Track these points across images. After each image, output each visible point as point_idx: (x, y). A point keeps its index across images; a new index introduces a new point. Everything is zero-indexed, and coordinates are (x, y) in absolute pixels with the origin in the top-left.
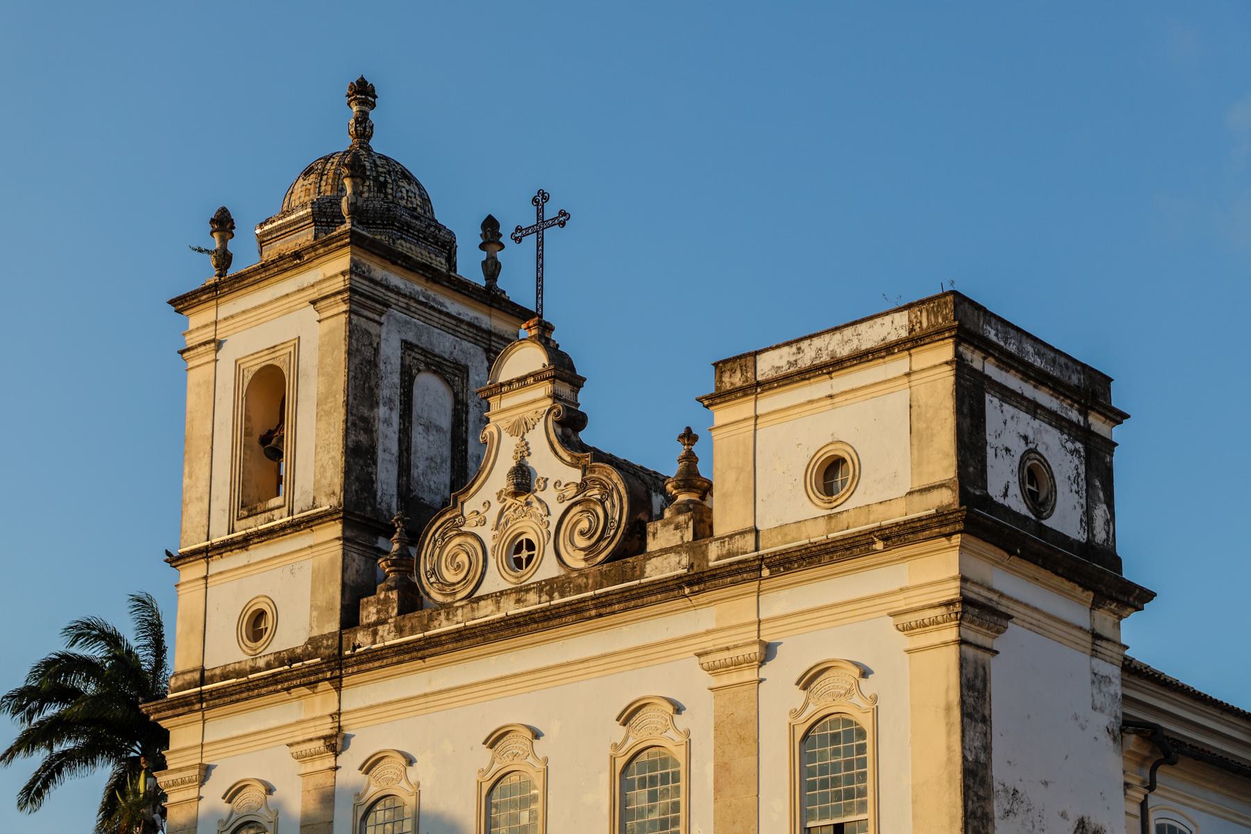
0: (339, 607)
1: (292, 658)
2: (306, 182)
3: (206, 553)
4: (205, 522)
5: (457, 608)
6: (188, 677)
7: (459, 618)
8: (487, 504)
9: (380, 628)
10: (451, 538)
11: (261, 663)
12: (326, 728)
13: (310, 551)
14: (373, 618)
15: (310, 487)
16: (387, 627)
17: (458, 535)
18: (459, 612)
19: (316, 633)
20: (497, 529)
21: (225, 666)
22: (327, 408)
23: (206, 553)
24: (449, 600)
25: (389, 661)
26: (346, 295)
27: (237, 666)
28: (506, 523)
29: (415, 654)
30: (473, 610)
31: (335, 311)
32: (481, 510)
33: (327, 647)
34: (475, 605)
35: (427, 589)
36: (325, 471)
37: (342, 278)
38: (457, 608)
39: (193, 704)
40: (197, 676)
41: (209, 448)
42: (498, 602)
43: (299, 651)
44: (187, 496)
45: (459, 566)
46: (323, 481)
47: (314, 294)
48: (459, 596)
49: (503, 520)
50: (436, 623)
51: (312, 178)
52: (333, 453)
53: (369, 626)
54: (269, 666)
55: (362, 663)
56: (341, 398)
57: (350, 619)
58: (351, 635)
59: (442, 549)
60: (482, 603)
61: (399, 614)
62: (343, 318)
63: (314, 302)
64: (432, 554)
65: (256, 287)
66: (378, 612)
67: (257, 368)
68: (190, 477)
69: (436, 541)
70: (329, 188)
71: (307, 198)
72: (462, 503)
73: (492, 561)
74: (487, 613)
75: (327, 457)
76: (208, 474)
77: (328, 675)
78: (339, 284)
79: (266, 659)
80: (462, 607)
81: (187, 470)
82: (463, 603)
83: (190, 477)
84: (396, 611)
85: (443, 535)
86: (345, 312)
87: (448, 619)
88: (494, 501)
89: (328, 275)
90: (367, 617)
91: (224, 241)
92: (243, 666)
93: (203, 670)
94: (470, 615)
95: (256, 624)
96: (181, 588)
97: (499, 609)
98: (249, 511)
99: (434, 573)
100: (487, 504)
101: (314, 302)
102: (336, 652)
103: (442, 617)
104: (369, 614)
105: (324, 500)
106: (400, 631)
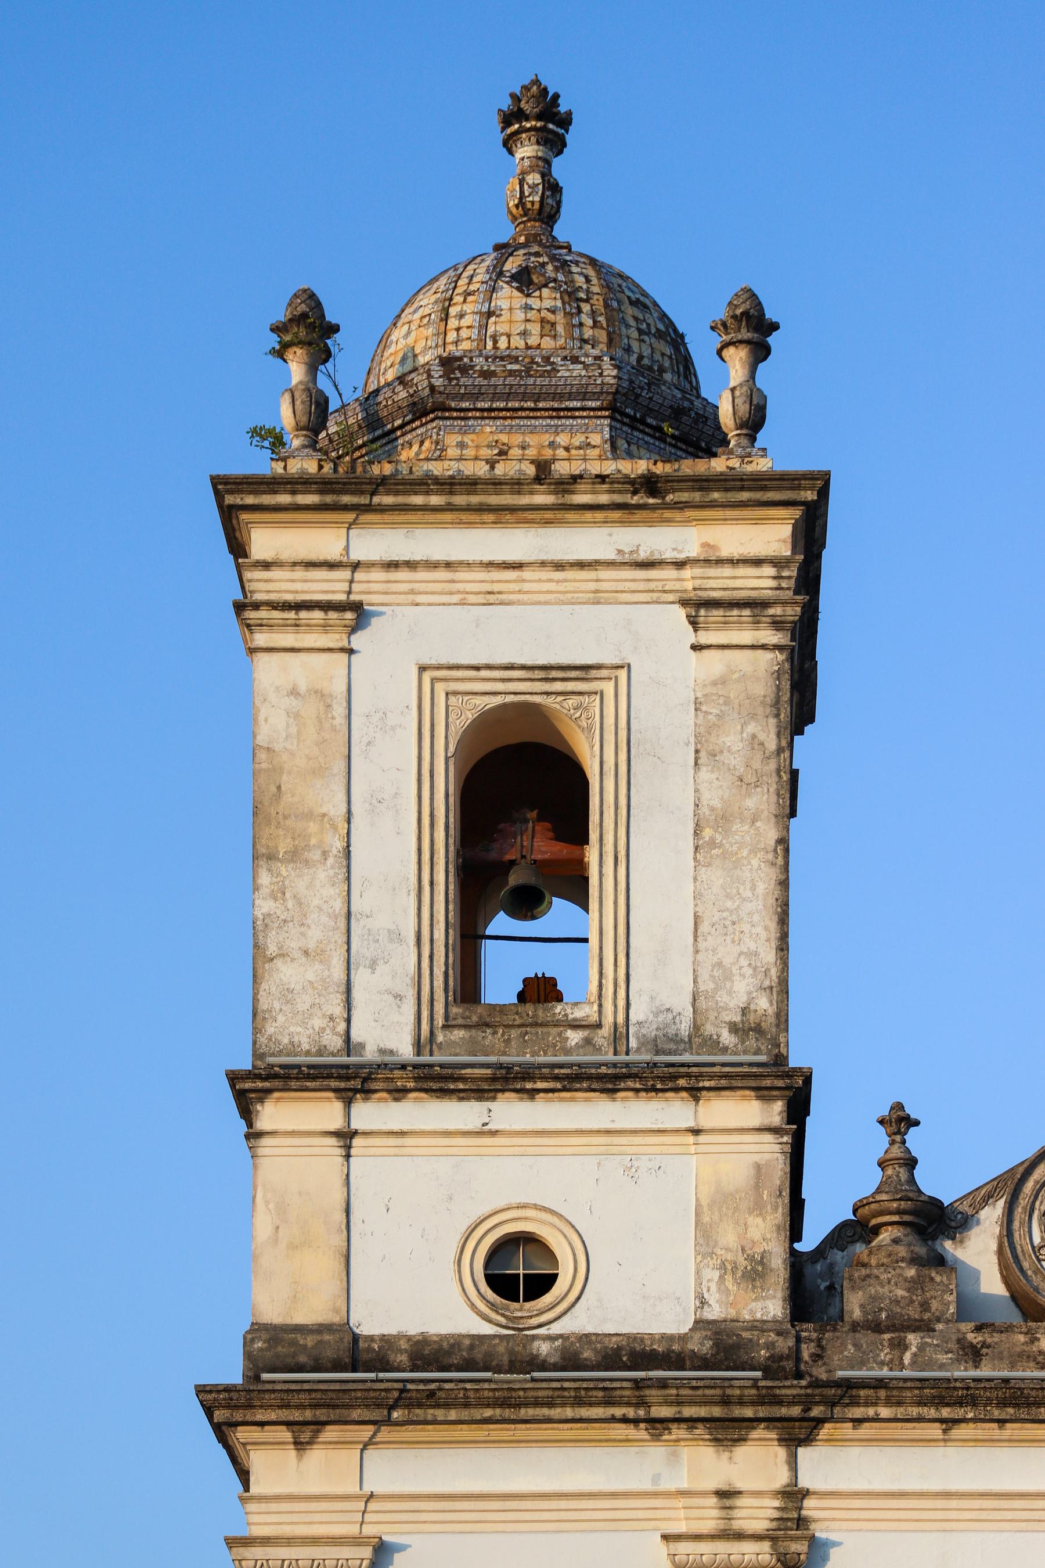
2: (534, 303)
3: (351, 1078)
4: (339, 1011)
15: (682, 1004)
23: (351, 1078)
31: (746, 637)
36: (728, 977)
46: (723, 998)
51: (548, 299)
70: (602, 335)
71: (548, 343)
75: (736, 950)
78: (760, 582)
91: (313, 369)
95: (517, 1269)
96: (265, 1141)
105: (727, 1038)
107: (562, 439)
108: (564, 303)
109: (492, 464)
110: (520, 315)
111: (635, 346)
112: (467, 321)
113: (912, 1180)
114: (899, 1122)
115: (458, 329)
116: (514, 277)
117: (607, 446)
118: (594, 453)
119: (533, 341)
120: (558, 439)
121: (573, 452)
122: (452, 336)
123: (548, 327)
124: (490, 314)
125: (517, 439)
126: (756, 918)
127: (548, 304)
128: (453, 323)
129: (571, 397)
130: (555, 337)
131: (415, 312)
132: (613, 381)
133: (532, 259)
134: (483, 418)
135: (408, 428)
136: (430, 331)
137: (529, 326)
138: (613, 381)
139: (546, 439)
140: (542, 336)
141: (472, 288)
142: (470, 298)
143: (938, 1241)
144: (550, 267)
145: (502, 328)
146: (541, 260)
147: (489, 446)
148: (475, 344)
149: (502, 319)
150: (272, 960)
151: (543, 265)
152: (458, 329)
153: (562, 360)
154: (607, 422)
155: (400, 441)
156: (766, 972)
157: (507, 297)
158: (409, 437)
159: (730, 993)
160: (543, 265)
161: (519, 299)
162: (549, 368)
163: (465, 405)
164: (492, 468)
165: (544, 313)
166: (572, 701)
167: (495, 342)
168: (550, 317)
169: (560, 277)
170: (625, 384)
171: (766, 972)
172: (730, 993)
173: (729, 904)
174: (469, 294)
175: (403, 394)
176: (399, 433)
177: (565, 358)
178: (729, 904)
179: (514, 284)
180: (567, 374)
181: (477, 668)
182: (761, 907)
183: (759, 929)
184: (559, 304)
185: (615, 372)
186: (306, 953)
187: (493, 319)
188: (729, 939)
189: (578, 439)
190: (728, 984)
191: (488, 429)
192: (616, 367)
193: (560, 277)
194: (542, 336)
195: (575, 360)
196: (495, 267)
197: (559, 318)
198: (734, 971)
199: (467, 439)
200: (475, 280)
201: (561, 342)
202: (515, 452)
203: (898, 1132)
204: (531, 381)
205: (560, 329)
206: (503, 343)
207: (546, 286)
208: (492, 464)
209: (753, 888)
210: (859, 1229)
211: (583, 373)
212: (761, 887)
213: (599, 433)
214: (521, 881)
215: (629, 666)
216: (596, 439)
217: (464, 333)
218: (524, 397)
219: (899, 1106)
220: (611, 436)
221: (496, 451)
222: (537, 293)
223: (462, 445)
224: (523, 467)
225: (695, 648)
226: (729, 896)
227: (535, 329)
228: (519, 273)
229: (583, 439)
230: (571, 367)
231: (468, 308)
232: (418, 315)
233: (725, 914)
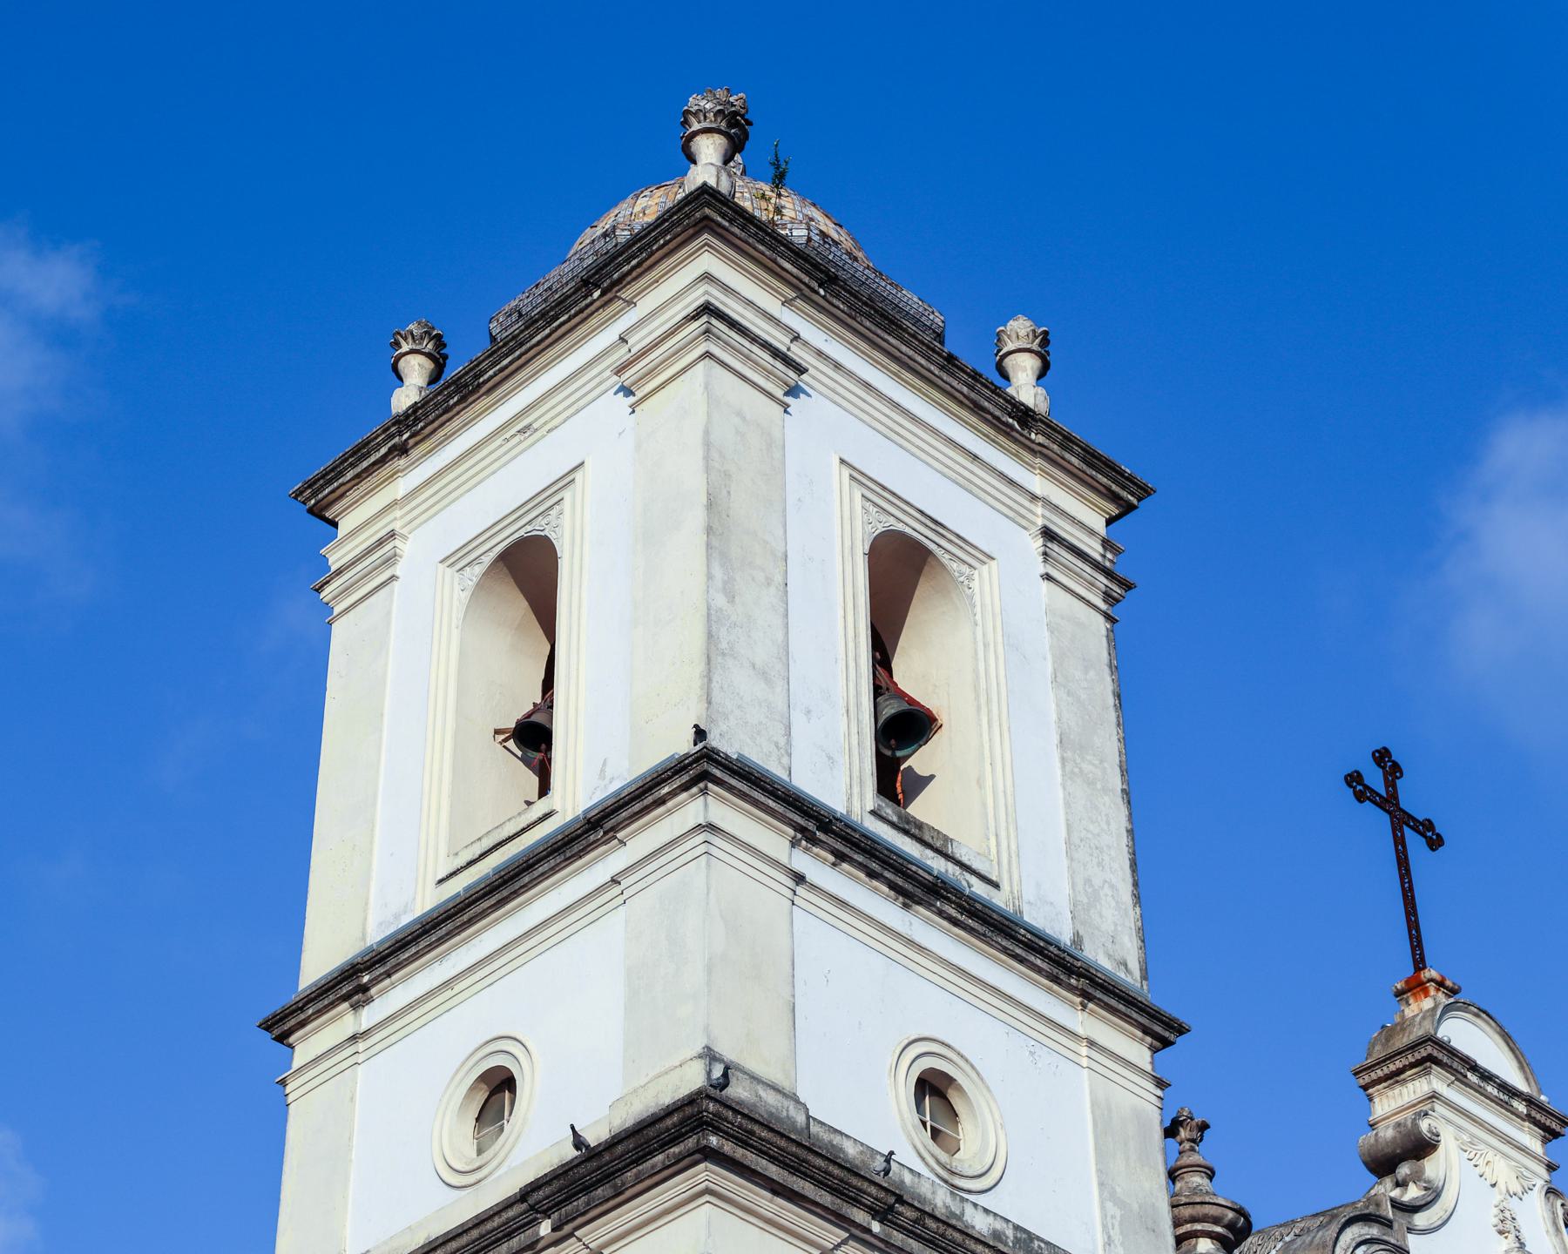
39: (856, 1202)
63: (1048, 534)
65: (894, 367)
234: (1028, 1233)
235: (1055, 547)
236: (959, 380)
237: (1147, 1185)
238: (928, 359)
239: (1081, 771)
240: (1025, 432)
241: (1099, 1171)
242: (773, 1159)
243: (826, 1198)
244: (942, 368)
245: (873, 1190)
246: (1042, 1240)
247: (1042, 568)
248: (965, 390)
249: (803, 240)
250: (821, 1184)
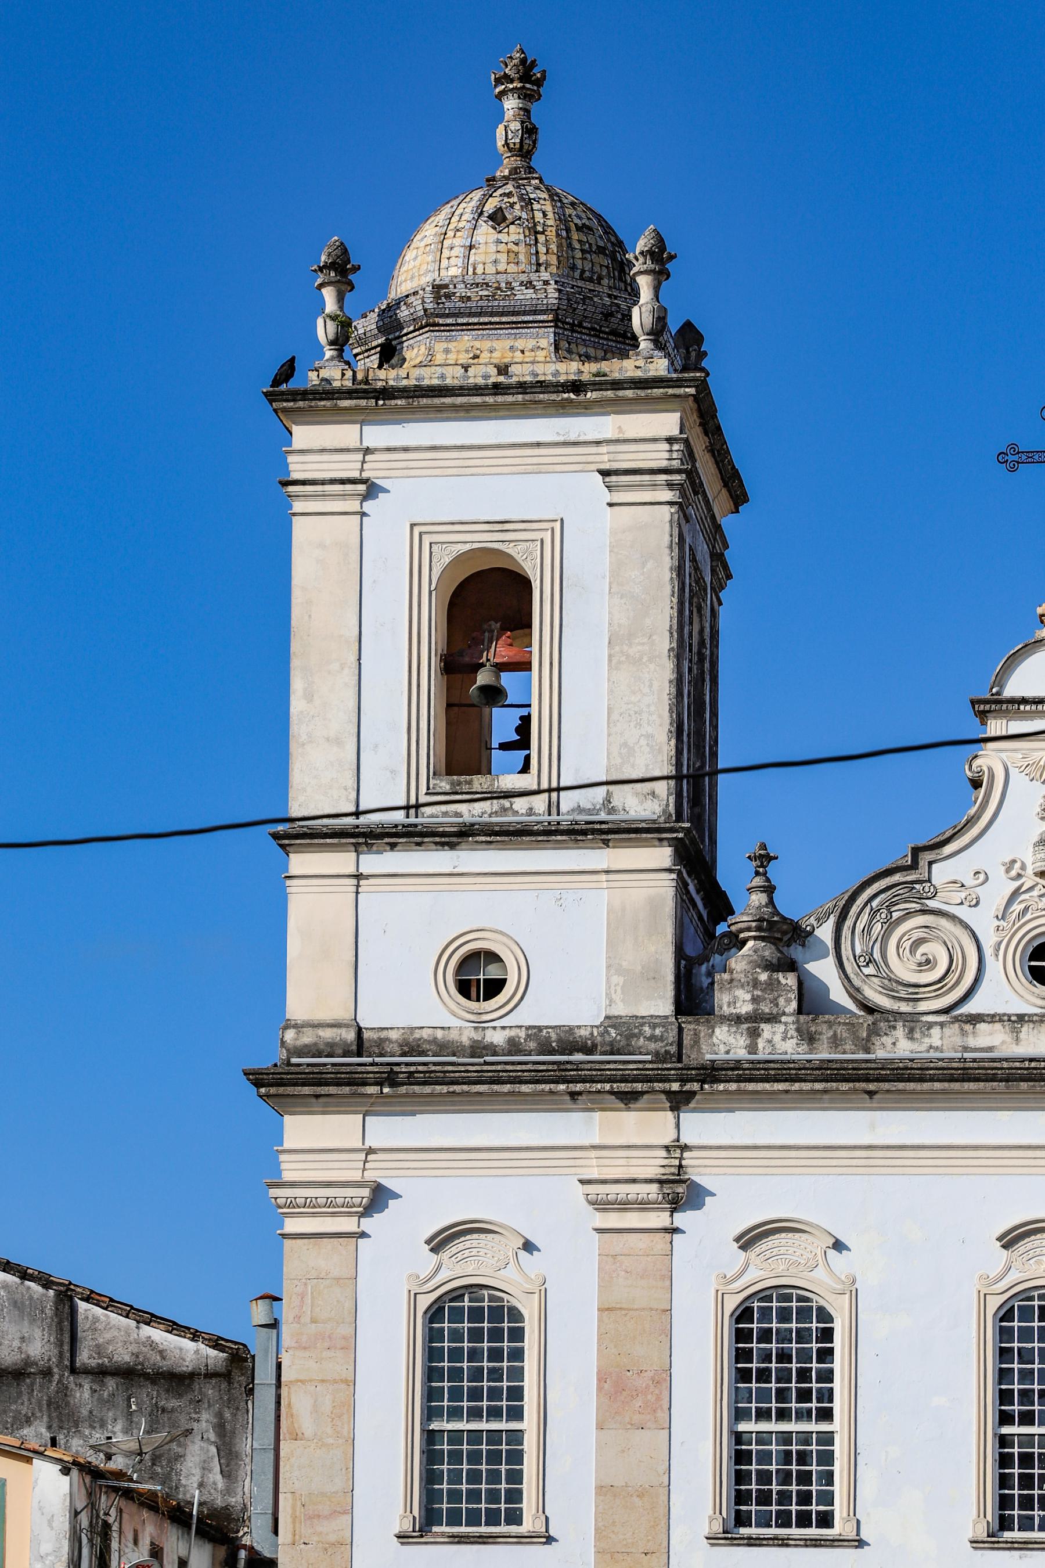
0: (670, 977)
1: (569, 1042)
2: (503, 237)
5: (930, 1025)
6: (327, 1034)
7: (936, 1042)
8: (983, 876)
9: (766, 1029)
10: (909, 915)
11: (497, 1038)
12: (653, 1165)
13: (604, 877)
14: (745, 1008)
16: (782, 1028)
17: (924, 912)
18: (936, 1031)
19: (620, 1010)
20: (1003, 918)
21: (412, 1029)
22: (633, 651)
24: (904, 1007)
25: (806, 1086)
26: (677, 478)
27: (439, 1034)
28: (1026, 909)
29: (863, 1085)
30: (963, 1033)
32: (969, 881)
33: (652, 1038)
34: (968, 1027)
35: (857, 982)
37: (666, 446)
38: (930, 1025)
40: (350, 1036)
41: (353, 658)
42: (1016, 1032)
43: (584, 1033)
44: (298, 729)
45: (928, 962)
47: (605, 458)
48: (923, 1006)
49: (1017, 907)
50: (887, 1040)
51: (515, 233)
52: (650, 730)
53: (738, 1020)
54: (514, 1046)
55: (750, 1080)
56: (664, 643)
57: (692, 999)
58: (703, 1030)
59: (891, 925)
60: (982, 1027)
61: (800, 1011)
62: (666, 512)
63: (605, 473)
64: (868, 929)
66: (755, 1000)
67: (468, 547)
68: (309, 697)
69: (874, 913)
71: (512, 268)
72: (930, 863)
73: (994, 967)
74: (993, 1041)
76: (352, 703)
77: (675, 1086)
79: (508, 1033)
80: (942, 1025)
81: (297, 684)
82: (942, 1018)
83: (309, 697)
84: (794, 1005)
85: (890, 906)
86: (671, 503)
87: (910, 1036)
88: (997, 874)
89: (630, 435)
90: (732, 1003)
92: (453, 1035)
93: (360, 1031)
94: (958, 1041)
97: (1017, 1040)
98: (452, 784)
99: (871, 961)
100: (983, 876)
101: (605, 473)
102: (673, 1049)
103: (900, 1032)
104: (734, 999)
106: (810, 1039)
107: (520, 344)
108: (525, 237)
109: (466, 368)
110: (493, 248)
111: (580, 266)
112: (454, 253)
113: (771, 902)
114: (764, 859)
115: (449, 258)
116: (491, 217)
117: (552, 349)
118: (541, 355)
119: (501, 267)
120: (516, 344)
121: (527, 354)
122: (445, 263)
123: (512, 255)
124: (471, 247)
125: (487, 345)
126: (652, 708)
127: (513, 238)
128: (446, 253)
129: (525, 313)
130: (517, 263)
131: (422, 239)
132: (556, 301)
133: (506, 200)
134: (462, 330)
135: (410, 336)
136: (430, 258)
137: (499, 256)
138: (556, 301)
139: (509, 343)
140: (508, 263)
141: (461, 225)
142: (458, 234)
143: (792, 947)
144: (517, 207)
145: (480, 258)
146: (511, 200)
147: (467, 351)
148: (460, 270)
149: (480, 251)
150: (303, 745)
151: (512, 205)
152: (449, 258)
153: (521, 284)
154: (552, 330)
155: (405, 344)
156: (660, 751)
157: (485, 232)
158: (411, 342)
159: (633, 766)
160: (512, 205)
161: (493, 236)
162: (509, 293)
163: (449, 321)
164: (466, 371)
165: (511, 246)
166: (522, 546)
167: (474, 269)
168: (515, 248)
169: (524, 215)
170: (565, 302)
171: (660, 751)
172: (633, 766)
173: (633, 699)
174: (458, 230)
175: (406, 313)
176: (405, 338)
177: (521, 284)
178: (633, 699)
179: (491, 223)
180: (522, 297)
181: (453, 523)
182: (656, 700)
183: (655, 717)
184: (522, 237)
185: (556, 295)
186: (328, 740)
187: (473, 251)
188: (632, 724)
189: (531, 343)
190: (632, 759)
191: (466, 338)
192: (560, 291)
193: (524, 215)
194: (508, 263)
195: (529, 284)
196: (478, 207)
197: (522, 249)
198: (636, 748)
199: (451, 346)
200: (463, 218)
201: (522, 267)
202: (485, 357)
203: (762, 866)
204: (496, 303)
205: (522, 257)
206: (480, 270)
207: (513, 223)
208: (466, 368)
209: (651, 686)
210: (734, 940)
211: (534, 296)
212: (656, 685)
213: (546, 339)
214: (483, 683)
215: (562, 520)
216: (544, 343)
217: (453, 261)
218: (492, 314)
219: (763, 846)
220: (555, 340)
221: (471, 355)
222: (506, 230)
223: (447, 351)
224: (488, 370)
225: (610, 505)
226: (634, 693)
227: (503, 258)
228: (495, 213)
229: (534, 343)
230: (525, 291)
231: (457, 242)
232: (423, 244)
233: (629, 706)
234: (534, 1027)
235: (614, 478)
236: (513, 394)
237: (653, 949)
238: (482, 395)
239: (628, 656)
240: (582, 397)
241: (608, 958)
242: (304, 1085)
243: (346, 1090)
244: (495, 394)
245: (371, 1075)
246: (547, 1027)
247: (608, 497)
248: (520, 397)
249: (422, 313)
250: (338, 1084)
